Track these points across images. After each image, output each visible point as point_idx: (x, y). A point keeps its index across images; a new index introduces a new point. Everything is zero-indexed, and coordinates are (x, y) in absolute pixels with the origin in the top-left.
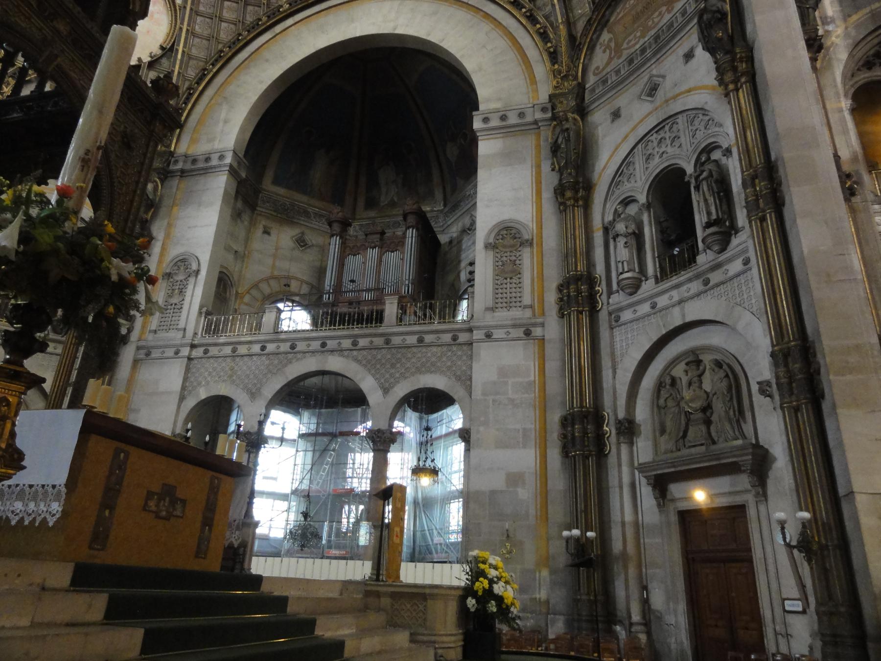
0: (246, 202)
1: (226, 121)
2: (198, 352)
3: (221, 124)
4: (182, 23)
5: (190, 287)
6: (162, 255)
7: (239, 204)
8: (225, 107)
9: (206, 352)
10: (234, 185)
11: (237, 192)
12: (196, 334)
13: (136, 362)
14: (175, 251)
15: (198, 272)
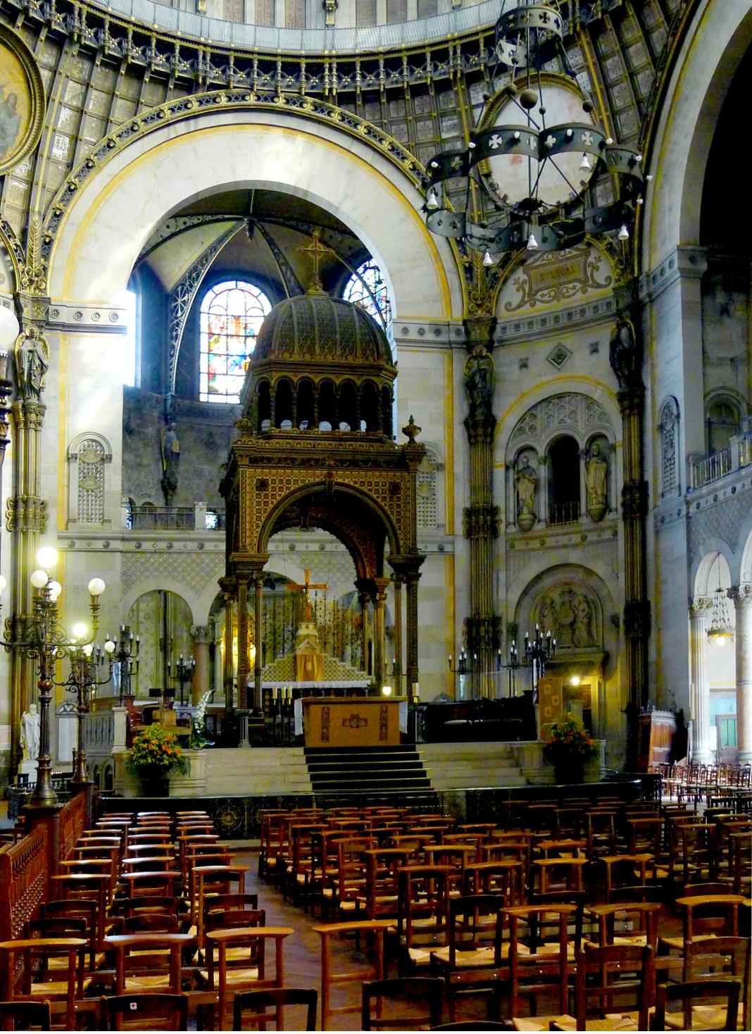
0: (729, 289)
1: (670, 210)
2: (693, 509)
3: (667, 213)
4: (600, 114)
5: (676, 437)
6: (653, 405)
7: (720, 298)
8: (666, 189)
9: (698, 506)
10: (696, 288)
11: (707, 288)
12: (688, 488)
13: (657, 533)
14: (660, 401)
15: (678, 416)
